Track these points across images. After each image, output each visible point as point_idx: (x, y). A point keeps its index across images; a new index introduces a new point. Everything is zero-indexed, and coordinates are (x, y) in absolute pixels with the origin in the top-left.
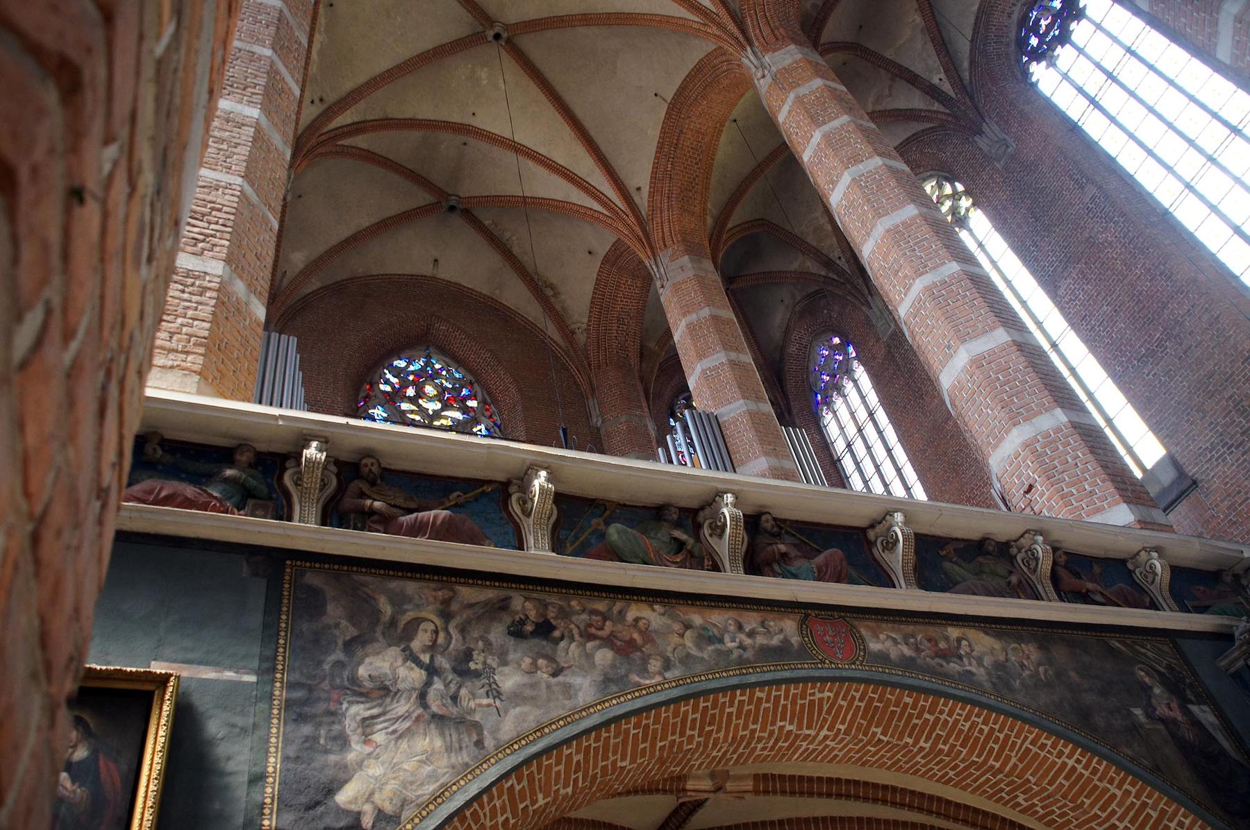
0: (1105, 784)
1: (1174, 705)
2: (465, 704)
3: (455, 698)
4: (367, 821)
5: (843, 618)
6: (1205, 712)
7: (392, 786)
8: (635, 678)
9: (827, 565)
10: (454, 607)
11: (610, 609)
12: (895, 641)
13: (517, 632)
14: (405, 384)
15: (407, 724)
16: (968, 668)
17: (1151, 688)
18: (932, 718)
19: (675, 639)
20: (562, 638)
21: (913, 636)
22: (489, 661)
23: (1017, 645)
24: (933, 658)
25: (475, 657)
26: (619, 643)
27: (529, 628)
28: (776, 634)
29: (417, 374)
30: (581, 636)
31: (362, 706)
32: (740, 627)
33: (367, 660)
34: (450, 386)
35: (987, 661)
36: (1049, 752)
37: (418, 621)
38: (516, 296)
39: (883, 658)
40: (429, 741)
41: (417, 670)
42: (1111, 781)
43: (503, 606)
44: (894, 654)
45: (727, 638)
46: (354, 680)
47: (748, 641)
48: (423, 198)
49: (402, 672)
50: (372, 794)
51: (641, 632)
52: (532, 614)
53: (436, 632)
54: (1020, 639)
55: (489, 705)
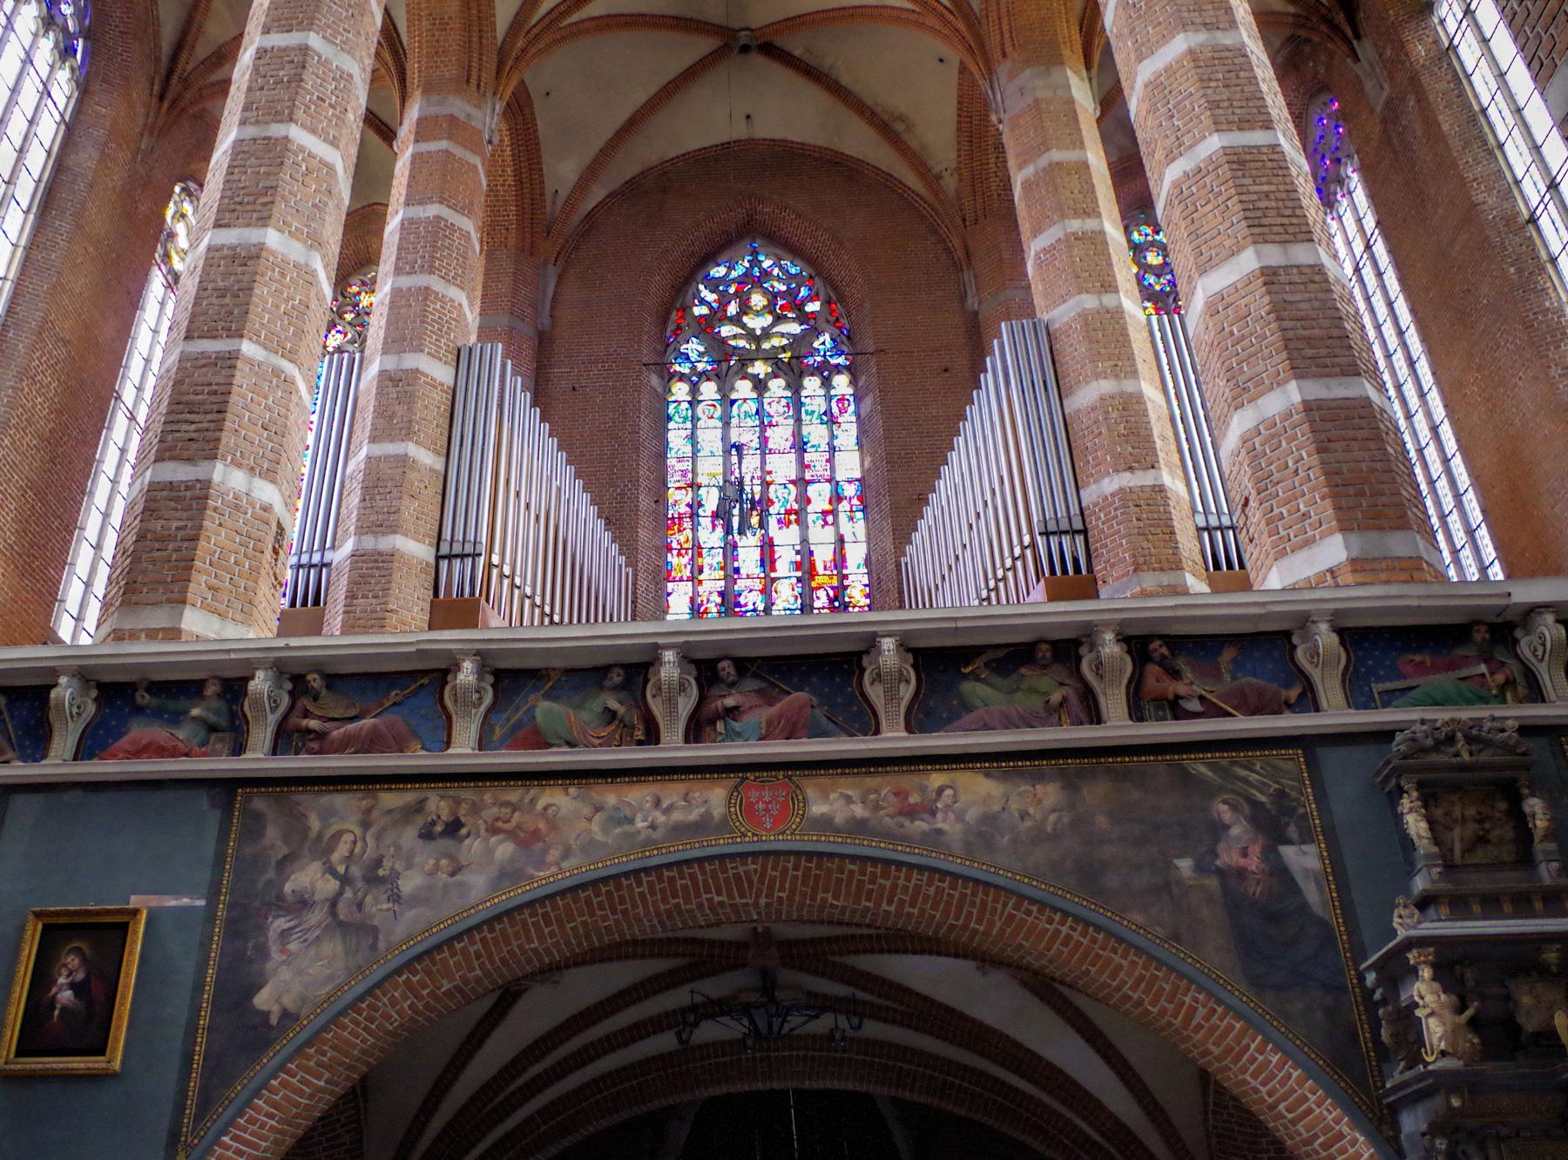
0: (1106, 954)
1: (1255, 850)
2: (367, 910)
3: (360, 905)
4: (274, 1020)
5: (789, 778)
6: (1305, 853)
8: (531, 871)
9: (780, 716)
10: (375, 814)
11: (522, 799)
12: (849, 799)
13: (427, 835)
14: (724, 302)
15: (317, 933)
16: (939, 825)
17: (1228, 827)
18: (888, 884)
19: (583, 824)
20: (469, 834)
21: (876, 791)
22: (396, 866)
23: (1029, 788)
24: (892, 817)
25: (385, 863)
26: (522, 835)
27: (439, 828)
28: (697, 807)
29: (741, 282)
30: (487, 830)
31: (283, 919)
32: (657, 803)
33: (293, 877)
34: (783, 288)
35: (972, 815)
36: (1036, 918)
37: (340, 834)
38: (858, 141)
39: (825, 823)
40: (333, 947)
41: (333, 881)
42: (1115, 951)
43: (419, 808)
44: (839, 819)
45: (639, 817)
46: (280, 897)
47: (660, 818)
48: (705, 45)
49: (320, 884)
50: (279, 997)
51: (548, 821)
53: (355, 843)
54: (1038, 778)
55: (388, 910)
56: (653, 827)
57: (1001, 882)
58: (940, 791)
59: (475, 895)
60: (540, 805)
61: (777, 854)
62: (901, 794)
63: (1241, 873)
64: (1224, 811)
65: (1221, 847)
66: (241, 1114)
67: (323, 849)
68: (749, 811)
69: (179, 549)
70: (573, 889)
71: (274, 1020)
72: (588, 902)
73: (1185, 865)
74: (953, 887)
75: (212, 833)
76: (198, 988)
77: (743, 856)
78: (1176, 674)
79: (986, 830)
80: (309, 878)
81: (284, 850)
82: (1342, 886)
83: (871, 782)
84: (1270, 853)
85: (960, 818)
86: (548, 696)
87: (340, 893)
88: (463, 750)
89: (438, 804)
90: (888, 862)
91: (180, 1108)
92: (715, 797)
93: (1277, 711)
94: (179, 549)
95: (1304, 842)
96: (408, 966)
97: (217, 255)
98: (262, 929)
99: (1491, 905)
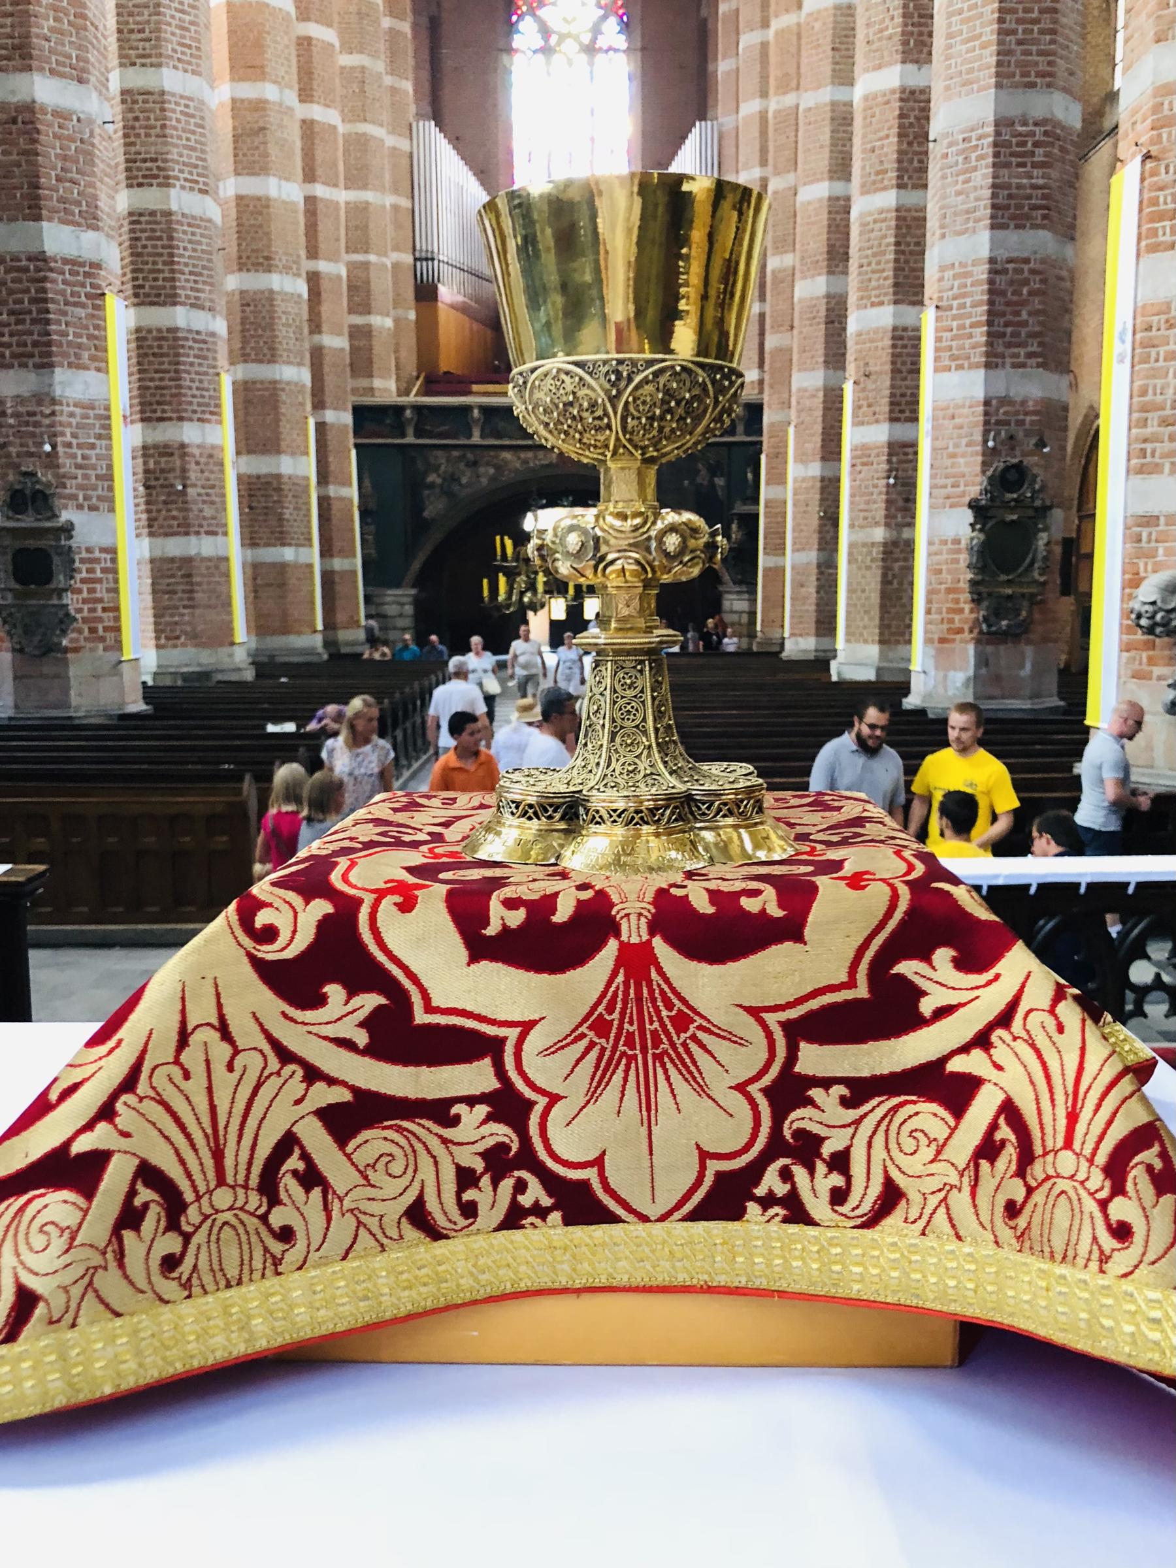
13: (467, 465)
64: (700, 466)
67: (436, 469)
80: (432, 478)
88: (476, 439)
89: (470, 456)
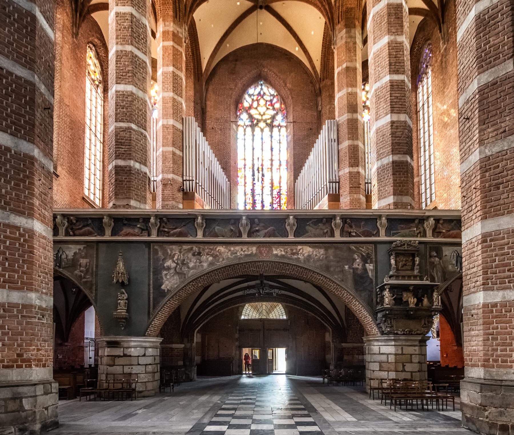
1: (361, 264)
3: (181, 269)
4: (166, 291)
7: (170, 285)
10: (182, 250)
12: (281, 251)
13: (194, 255)
17: (356, 260)
21: (287, 249)
32: (242, 250)
35: (306, 255)
37: (175, 254)
39: (276, 255)
43: (191, 249)
44: (279, 254)
46: (164, 267)
49: (172, 265)
52: (197, 251)
54: (321, 248)
56: (241, 255)
57: (310, 268)
58: (300, 249)
59: (205, 268)
60: (217, 250)
61: (266, 261)
62: (292, 250)
63: (357, 269)
65: (354, 263)
66: (162, 308)
68: (261, 252)
69: (126, 184)
70: (225, 267)
71: (166, 291)
72: (228, 269)
73: (347, 267)
74: (301, 269)
75: (147, 253)
76: (149, 285)
77: (259, 262)
78: (351, 227)
79: (309, 258)
80: (169, 263)
81: (163, 257)
82: (376, 273)
83: (286, 247)
84: (364, 266)
85: (303, 255)
86: (218, 226)
87: (177, 266)
88: (200, 237)
89: (195, 248)
90: (288, 264)
91: (149, 307)
92: (254, 249)
93: (371, 237)
94: (126, 184)
95: (370, 263)
96: (192, 281)
97: (119, 94)
98: (161, 274)
99: (404, 277)
